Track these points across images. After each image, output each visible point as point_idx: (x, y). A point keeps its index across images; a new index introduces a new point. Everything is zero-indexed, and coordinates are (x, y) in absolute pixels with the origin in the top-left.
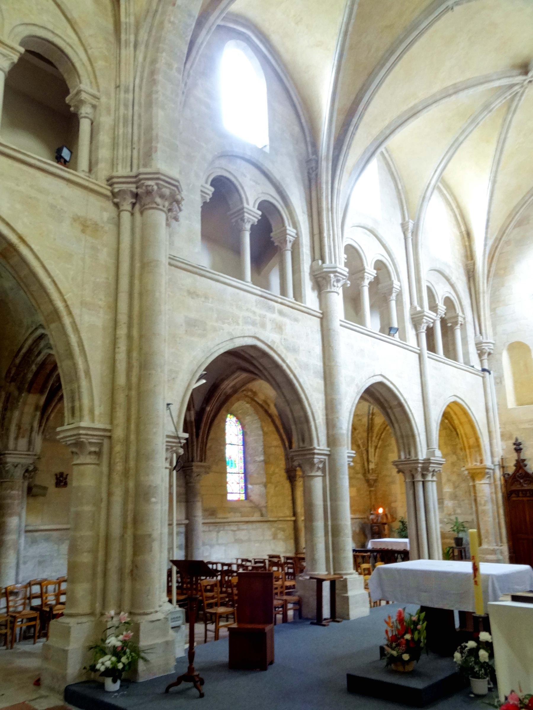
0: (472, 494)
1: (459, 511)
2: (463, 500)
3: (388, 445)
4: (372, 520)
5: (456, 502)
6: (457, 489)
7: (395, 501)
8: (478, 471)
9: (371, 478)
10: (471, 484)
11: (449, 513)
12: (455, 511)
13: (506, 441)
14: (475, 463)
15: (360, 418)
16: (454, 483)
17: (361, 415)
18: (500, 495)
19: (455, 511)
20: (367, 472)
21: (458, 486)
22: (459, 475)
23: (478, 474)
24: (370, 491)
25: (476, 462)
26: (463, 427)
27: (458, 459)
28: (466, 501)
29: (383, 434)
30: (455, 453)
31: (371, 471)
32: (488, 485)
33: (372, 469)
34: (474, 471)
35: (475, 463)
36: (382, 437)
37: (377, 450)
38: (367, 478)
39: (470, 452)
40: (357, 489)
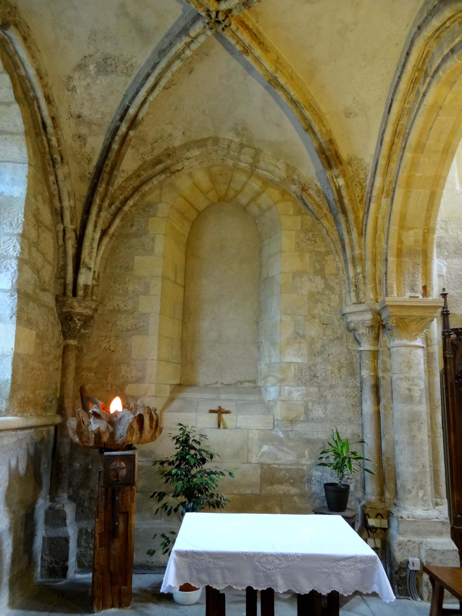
0: (366, 373)
1: (318, 412)
2: (332, 387)
3: (136, 235)
4: (98, 434)
5: (313, 390)
6: (319, 360)
7: (139, 380)
8: (416, 313)
9: (78, 310)
10: (366, 346)
11: (292, 415)
12: (307, 411)
13: (447, 258)
14: (408, 294)
15: (84, 130)
16: (312, 342)
17: (90, 124)
18: (437, 380)
19: (307, 411)
20: (70, 293)
21: (322, 352)
22: (325, 324)
23: (413, 321)
24: (66, 348)
25: (413, 289)
26: (407, 196)
27: (328, 286)
28: (339, 390)
29: (131, 203)
30: (320, 272)
31: (80, 293)
32: (422, 349)
33: (86, 287)
34: (405, 313)
35: (408, 294)
36: (126, 208)
37: (106, 240)
38: (65, 310)
39: (399, 265)
40: (38, 336)
